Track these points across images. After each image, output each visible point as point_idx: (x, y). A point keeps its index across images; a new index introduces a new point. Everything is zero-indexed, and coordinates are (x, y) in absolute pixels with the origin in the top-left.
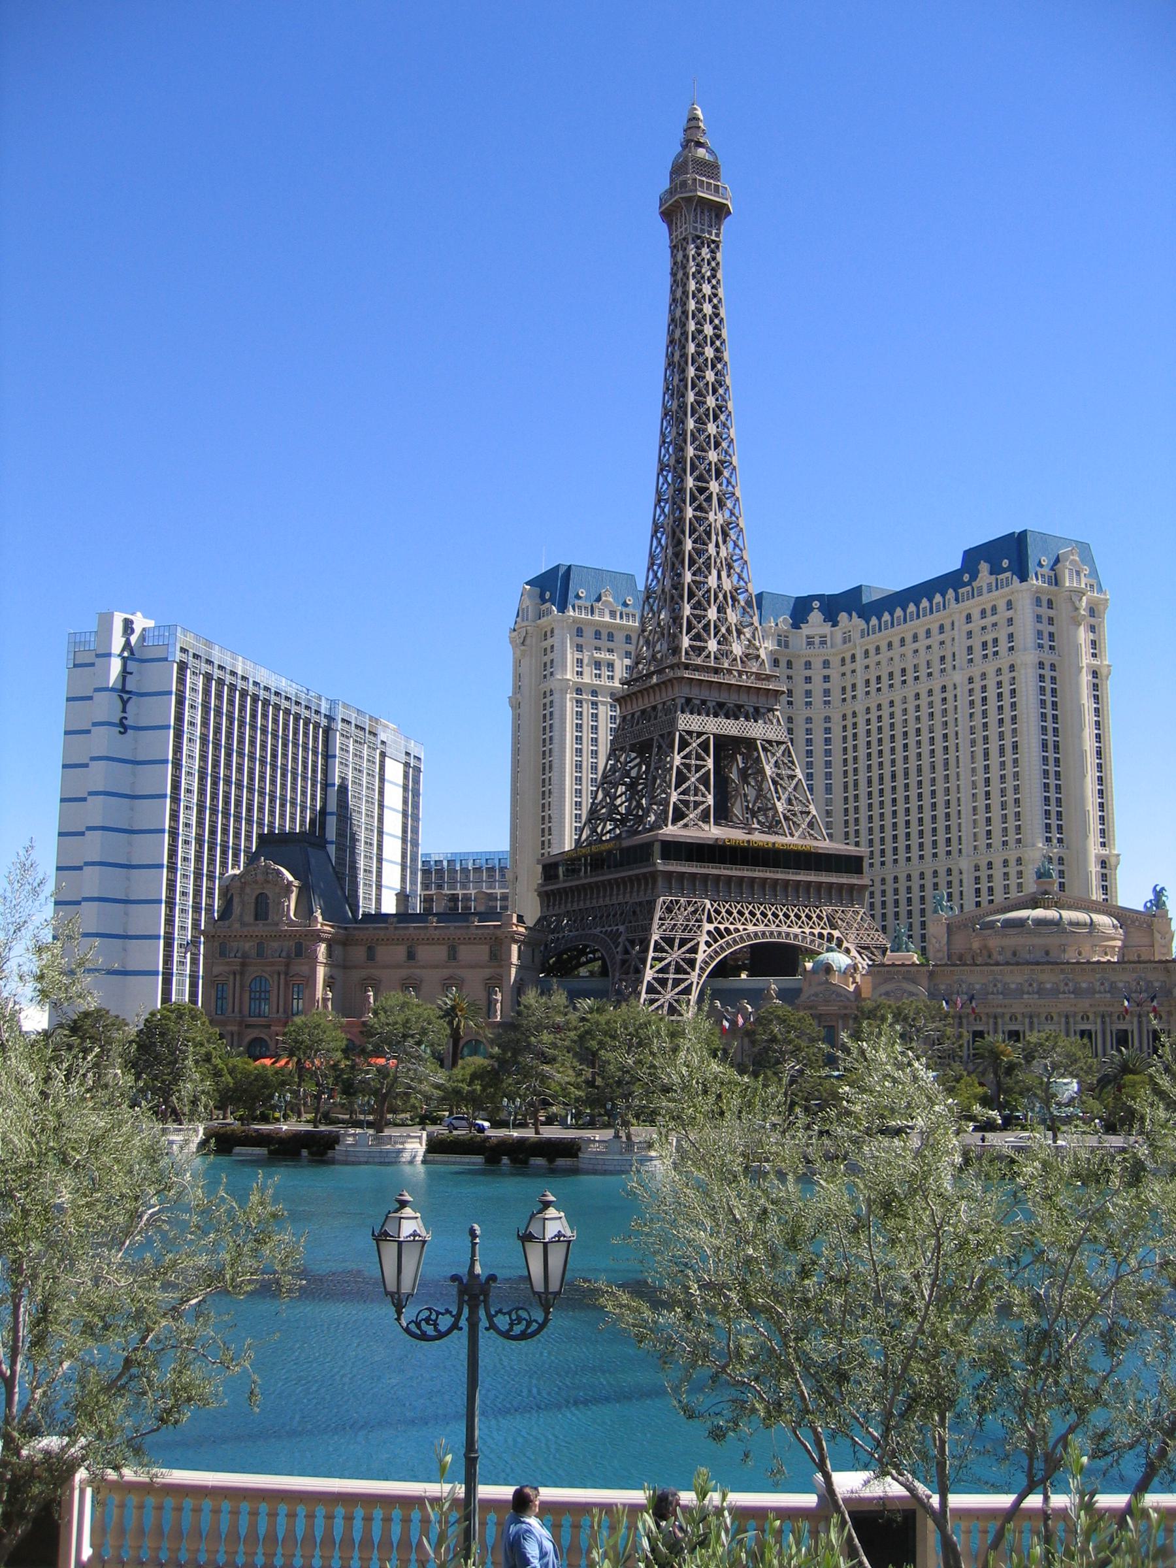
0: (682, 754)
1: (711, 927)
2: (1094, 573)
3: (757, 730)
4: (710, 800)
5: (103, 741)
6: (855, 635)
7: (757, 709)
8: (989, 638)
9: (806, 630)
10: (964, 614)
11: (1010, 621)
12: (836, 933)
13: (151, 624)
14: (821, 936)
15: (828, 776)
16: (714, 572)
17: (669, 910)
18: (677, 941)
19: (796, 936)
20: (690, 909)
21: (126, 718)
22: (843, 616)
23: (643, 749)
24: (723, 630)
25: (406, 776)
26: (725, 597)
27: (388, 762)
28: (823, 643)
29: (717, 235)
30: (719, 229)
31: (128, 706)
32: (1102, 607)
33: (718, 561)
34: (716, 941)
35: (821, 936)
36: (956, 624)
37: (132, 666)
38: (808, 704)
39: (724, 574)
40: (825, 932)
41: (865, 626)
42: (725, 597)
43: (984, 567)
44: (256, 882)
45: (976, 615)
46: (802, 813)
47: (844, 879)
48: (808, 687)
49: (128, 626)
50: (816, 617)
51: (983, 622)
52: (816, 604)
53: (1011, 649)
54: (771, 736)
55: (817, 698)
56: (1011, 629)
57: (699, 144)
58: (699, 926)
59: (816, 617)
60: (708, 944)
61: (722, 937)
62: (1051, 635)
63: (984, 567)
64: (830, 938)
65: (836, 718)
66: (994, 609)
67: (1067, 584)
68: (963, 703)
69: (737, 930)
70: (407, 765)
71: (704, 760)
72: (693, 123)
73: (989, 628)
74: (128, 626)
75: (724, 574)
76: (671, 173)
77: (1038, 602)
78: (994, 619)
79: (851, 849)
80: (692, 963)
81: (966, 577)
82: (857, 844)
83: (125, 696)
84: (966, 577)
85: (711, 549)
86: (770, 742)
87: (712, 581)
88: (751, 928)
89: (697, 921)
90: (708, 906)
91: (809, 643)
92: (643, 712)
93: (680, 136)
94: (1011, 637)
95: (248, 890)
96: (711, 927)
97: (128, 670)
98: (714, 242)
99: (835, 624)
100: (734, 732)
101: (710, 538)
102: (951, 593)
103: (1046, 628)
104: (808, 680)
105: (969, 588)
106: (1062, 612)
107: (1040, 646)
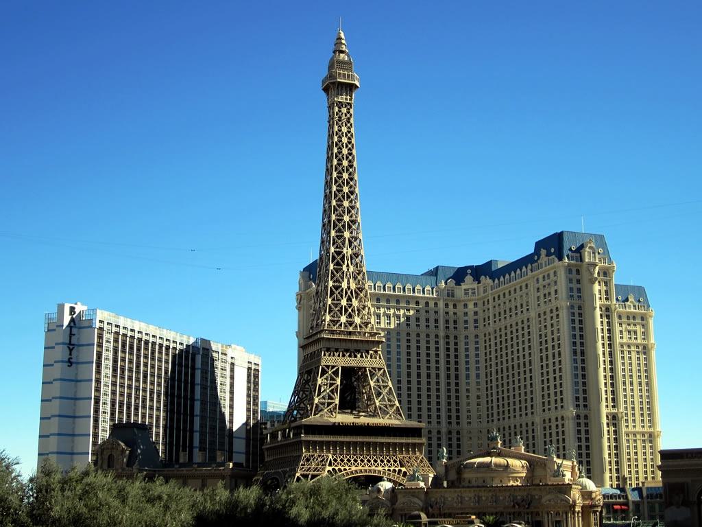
1: (330, 468)
2: (606, 252)
3: (367, 362)
4: (337, 401)
5: (58, 370)
6: (489, 289)
9: (464, 286)
10: (536, 278)
12: (404, 469)
13: (85, 308)
14: (394, 471)
15: (478, 368)
16: (346, 280)
17: (308, 460)
18: (310, 476)
19: (380, 472)
20: (319, 460)
21: (71, 358)
23: (309, 372)
24: (350, 310)
26: (351, 292)
28: (473, 293)
29: (351, 100)
30: (351, 96)
31: (73, 352)
32: (611, 271)
35: (394, 471)
37: (75, 331)
38: (466, 328)
40: (397, 469)
42: (351, 292)
43: (543, 252)
44: (108, 449)
45: (541, 277)
46: (390, 406)
47: (410, 440)
48: (466, 318)
49: (72, 310)
50: (469, 279)
51: (544, 283)
52: (469, 271)
54: (375, 365)
57: (342, 52)
59: (469, 279)
63: (543, 252)
64: (400, 471)
65: (481, 336)
66: (548, 275)
67: (587, 261)
69: (345, 470)
71: (334, 380)
72: (339, 41)
74: (72, 310)
75: (351, 280)
76: (329, 68)
77: (570, 271)
79: (413, 424)
81: (536, 258)
83: (71, 347)
84: (536, 258)
85: (344, 268)
86: (374, 369)
89: (323, 465)
90: (331, 457)
91: (466, 294)
93: (333, 47)
94: (556, 291)
95: (105, 453)
96: (330, 468)
97: (73, 333)
98: (348, 103)
99: (479, 282)
100: (353, 365)
101: (344, 262)
102: (529, 266)
103: (574, 285)
105: (536, 264)
106: (585, 276)
107: (572, 296)
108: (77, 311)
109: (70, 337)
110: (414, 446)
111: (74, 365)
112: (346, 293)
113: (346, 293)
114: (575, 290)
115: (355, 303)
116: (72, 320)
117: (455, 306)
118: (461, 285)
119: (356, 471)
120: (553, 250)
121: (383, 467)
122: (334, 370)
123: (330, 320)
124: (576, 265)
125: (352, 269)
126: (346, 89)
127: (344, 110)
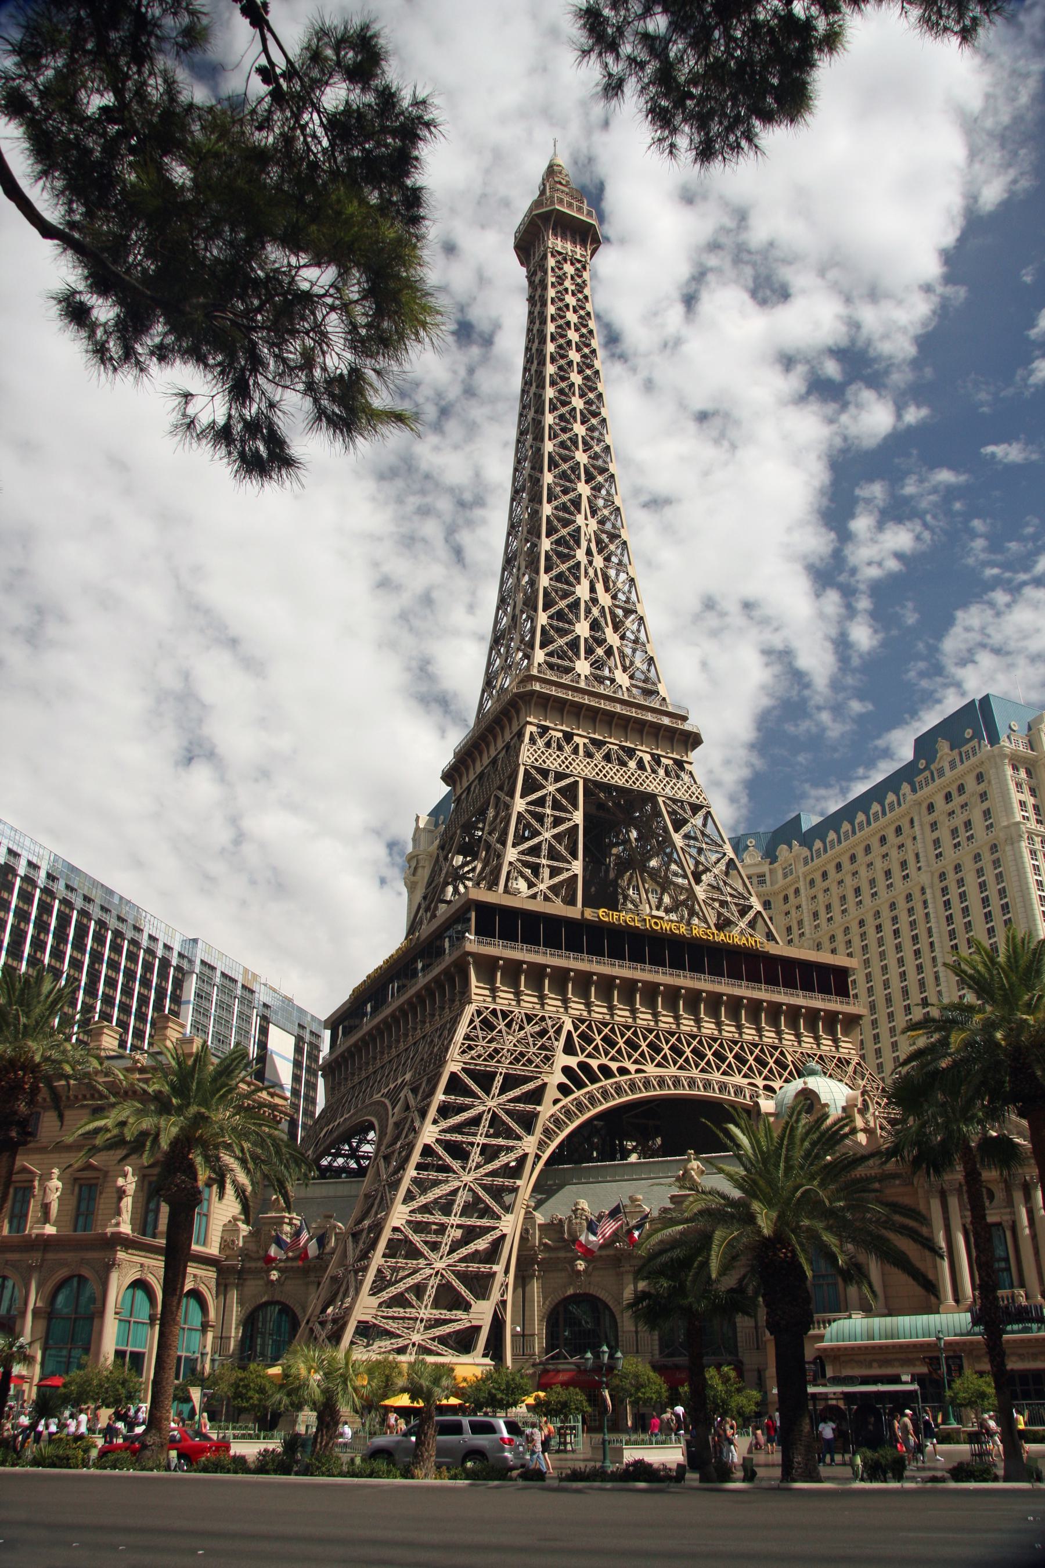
0: (529, 799)
1: (572, 1062)
7: (657, 759)
8: (958, 821)
10: (925, 805)
11: (984, 796)
19: (739, 1091)
22: (783, 850)
25: (298, 1050)
27: (272, 1028)
33: (591, 572)
34: (580, 1085)
36: (916, 819)
39: (600, 587)
41: (808, 853)
53: (989, 827)
56: (985, 805)
58: (547, 1058)
60: (564, 1089)
61: (594, 1080)
68: (935, 908)
69: (623, 1071)
70: (299, 1039)
73: (958, 811)
75: (600, 587)
78: (963, 799)
80: (528, 1122)
82: (833, 951)
84: (922, 764)
85: (580, 555)
87: (582, 591)
88: (651, 1070)
89: (543, 1047)
92: (481, 776)
94: (987, 814)
96: (572, 1062)
102: (906, 788)
105: (927, 773)
110: (831, 1020)
112: (588, 611)
113: (588, 611)
119: (661, 1082)
120: (968, 733)
121: (745, 1076)
122: (563, 783)
123: (546, 662)
125: (599, 561)
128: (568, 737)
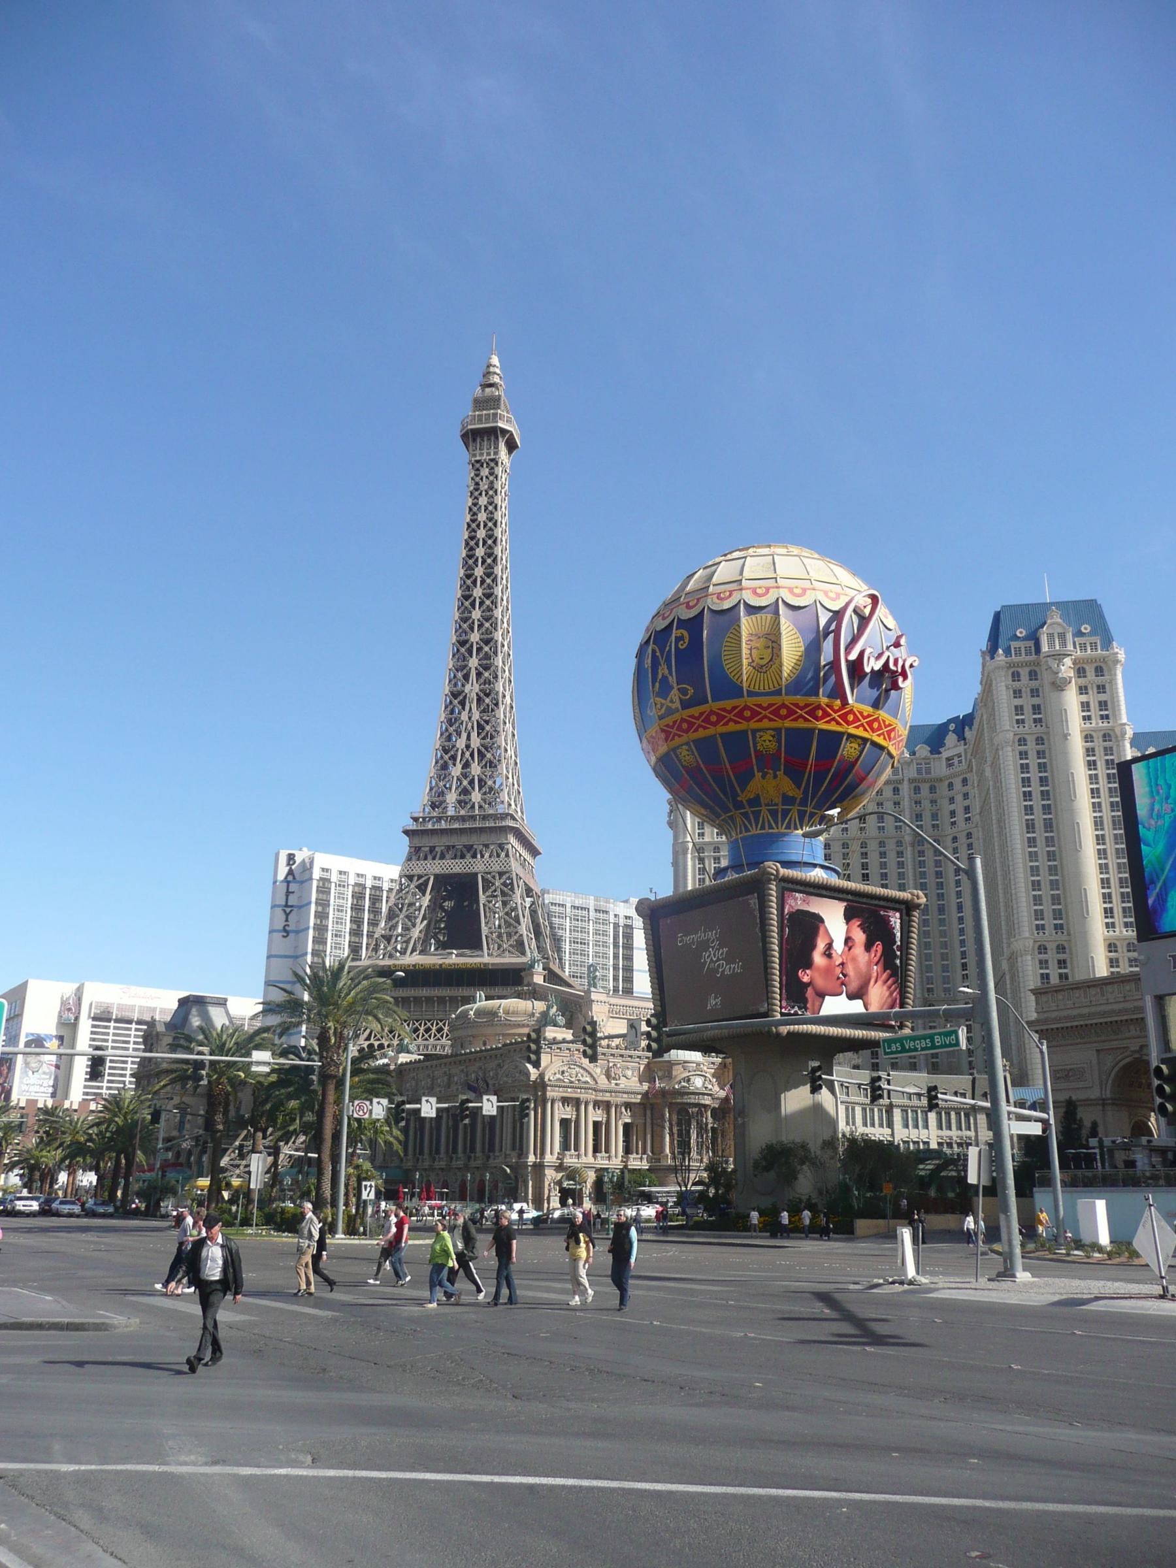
9: (945, 754)
24: (465, 783)
26: (472, 755)
37: (293, 887)
38: (953, 823)
39: (474, 735)
42: (472, 755)
49: (291, 858)
50: (951, 739)
52: (952, 726)
55: (960, 817)
59: (951, 739)
62: (1036, 709)
74: (291, 858)
75: (474, 735)
83: (288, 910)
91: (950, 765)
98: (492, 460)
103: (1027, 702)
104: (952, 800)
108: (298, 859)
109: (287, 896)
111: (292, 935)
112: (463, 754)
114: (1028, 709)
115: (476, 769)
116: (290, 872)
117: (932, 789)
118: (940, 753)
122: (421, 881)
124: (1027, 664)
125: (476, 715)
126: (489, 440)
127: (485, 472)
128: (432, 849)
